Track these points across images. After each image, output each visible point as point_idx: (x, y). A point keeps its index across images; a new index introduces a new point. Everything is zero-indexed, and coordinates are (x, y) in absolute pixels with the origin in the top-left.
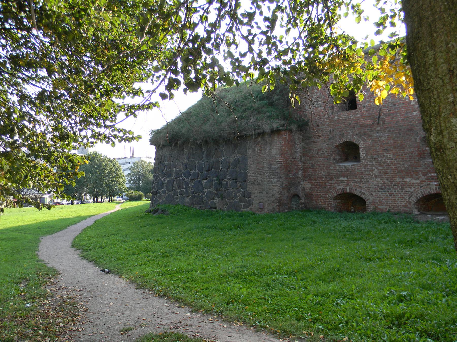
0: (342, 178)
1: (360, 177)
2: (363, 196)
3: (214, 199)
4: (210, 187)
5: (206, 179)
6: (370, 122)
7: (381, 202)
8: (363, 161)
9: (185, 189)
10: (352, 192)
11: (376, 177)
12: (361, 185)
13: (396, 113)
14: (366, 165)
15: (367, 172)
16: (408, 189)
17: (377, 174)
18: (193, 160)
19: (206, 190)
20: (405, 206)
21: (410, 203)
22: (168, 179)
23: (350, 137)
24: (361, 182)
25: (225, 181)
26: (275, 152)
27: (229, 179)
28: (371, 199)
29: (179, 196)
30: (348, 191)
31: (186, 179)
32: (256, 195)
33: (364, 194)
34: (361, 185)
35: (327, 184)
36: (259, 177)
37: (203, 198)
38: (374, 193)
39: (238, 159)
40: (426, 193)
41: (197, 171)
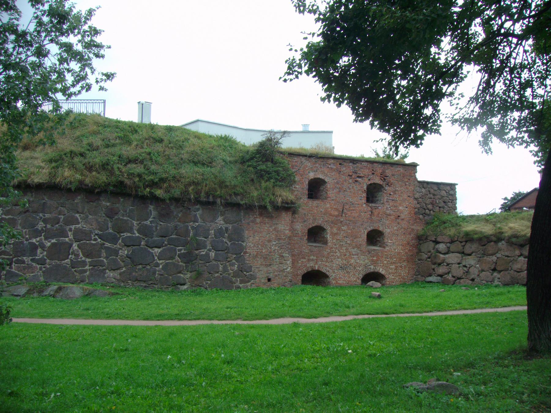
0: (312, 257)
1: (326, 258)
2: (327, 273)
3: (180, 272)
4: (172, 258)
5: (159, 248)
6: (336, 213)
7: (340, 278)
8: (329, 244)
9: (107, 258)
10: (320, 269)
11: (338, 258)
12: (327, 264)
13: (353, 210)
14: (332, 248)
15: (332, 254)
16: (358, 268)
17: (339, 255)
18: (125, 218)
19: (161, 261)
20: (356, 281)
21: (358, 278)
22: (54, 241)
23: (319, 222)
24: (327, 261)
25: (203, 251)
26: (283, 228)
27: (210, 250)
28: (334, 275)
29: (87, 267)
30: (317, 269)
31: (108, 245)
32: (261, 269)
33: (329, 271)
34: (327, 264)
35: (300, 262)
36: (264, 251)
37: (155, 271)
38: (336, 271)
39: (227, 229)
40: (369, 272)
41: (137, 235)
